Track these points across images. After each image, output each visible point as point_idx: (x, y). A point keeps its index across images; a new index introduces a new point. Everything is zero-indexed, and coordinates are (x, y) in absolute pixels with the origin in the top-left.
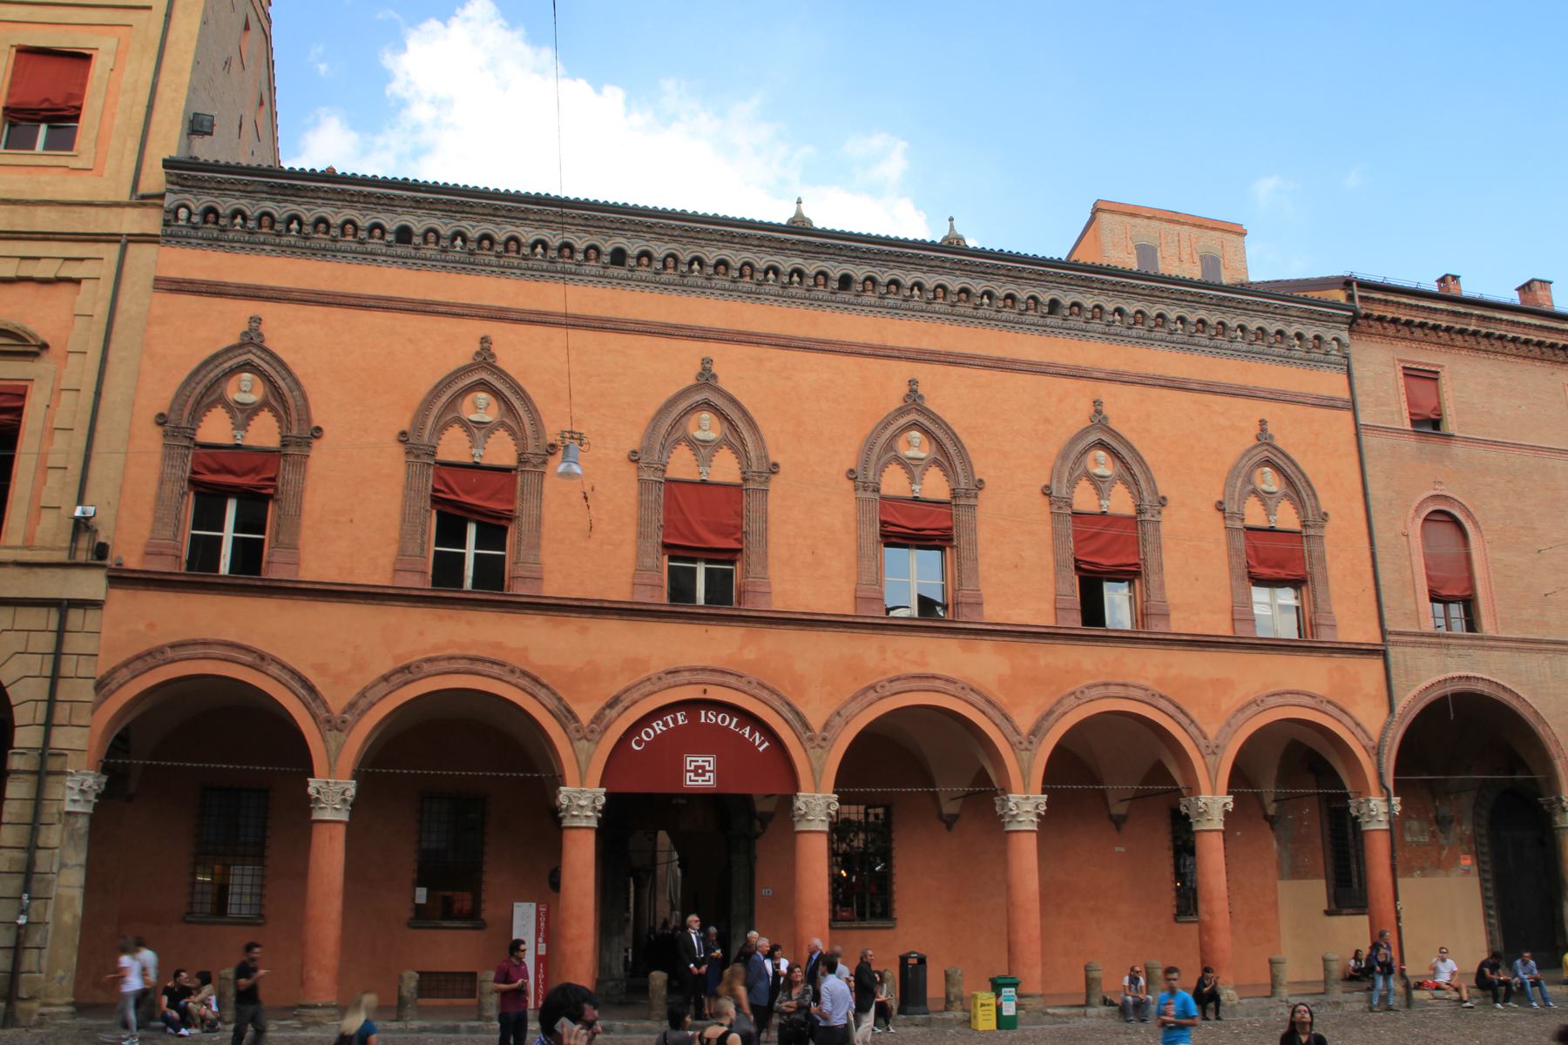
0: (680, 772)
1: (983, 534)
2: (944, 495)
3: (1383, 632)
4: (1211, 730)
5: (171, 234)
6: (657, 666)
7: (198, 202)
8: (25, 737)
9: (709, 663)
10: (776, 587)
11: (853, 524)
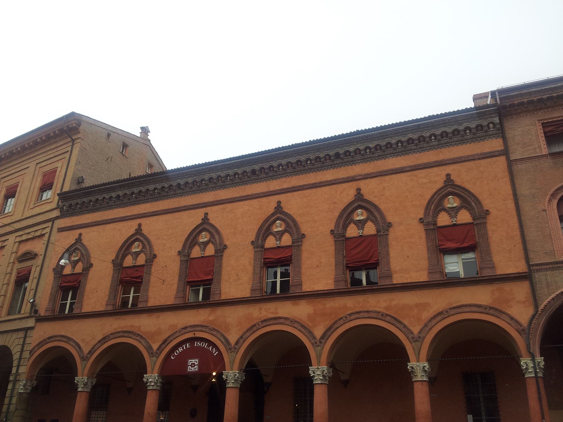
0: (187, 365)
1: (304, 255)
2: (289, 243)
3: (529, 266)
4: (416, 330)
6: (180, 326)
7: (67, 204)
8: (14, 370)
9: (197, 323)
10: (223, 291)
11: (252, 262)
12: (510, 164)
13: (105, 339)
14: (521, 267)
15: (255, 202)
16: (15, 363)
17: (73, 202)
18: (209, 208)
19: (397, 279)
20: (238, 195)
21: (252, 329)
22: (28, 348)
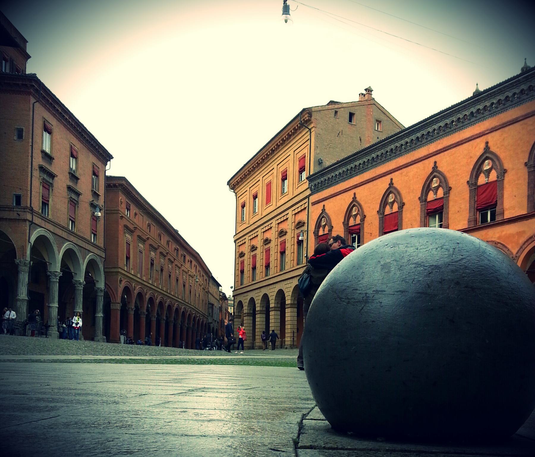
1: (451, 204)
15: (420, 164)
18: (393, 174)
20: (410, 161)
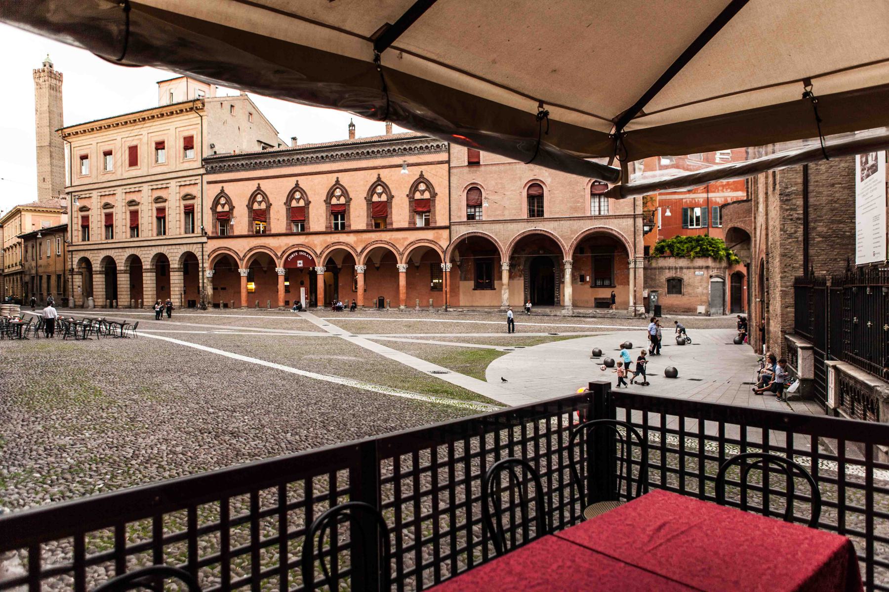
1: (352, 210)
4: (401, 250)
5: (208, 173)
7: (210, 166)
8: (201, 265)
12: (450, 168)
13: (251, 250)
14: (447, 224)
16: (200, 261)
17: (214, 165)
19: (395, 226)
21: (327, 247)
22: (206, 254)
